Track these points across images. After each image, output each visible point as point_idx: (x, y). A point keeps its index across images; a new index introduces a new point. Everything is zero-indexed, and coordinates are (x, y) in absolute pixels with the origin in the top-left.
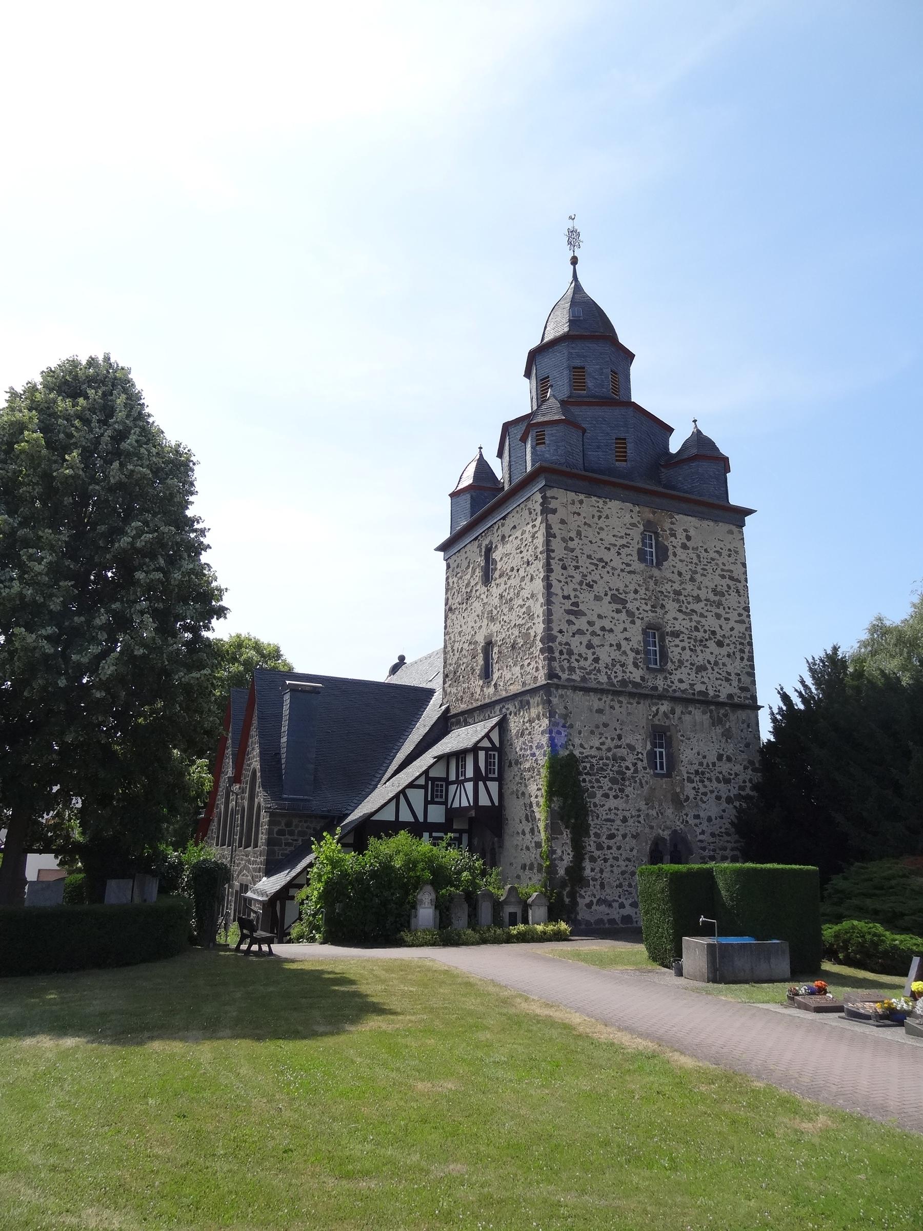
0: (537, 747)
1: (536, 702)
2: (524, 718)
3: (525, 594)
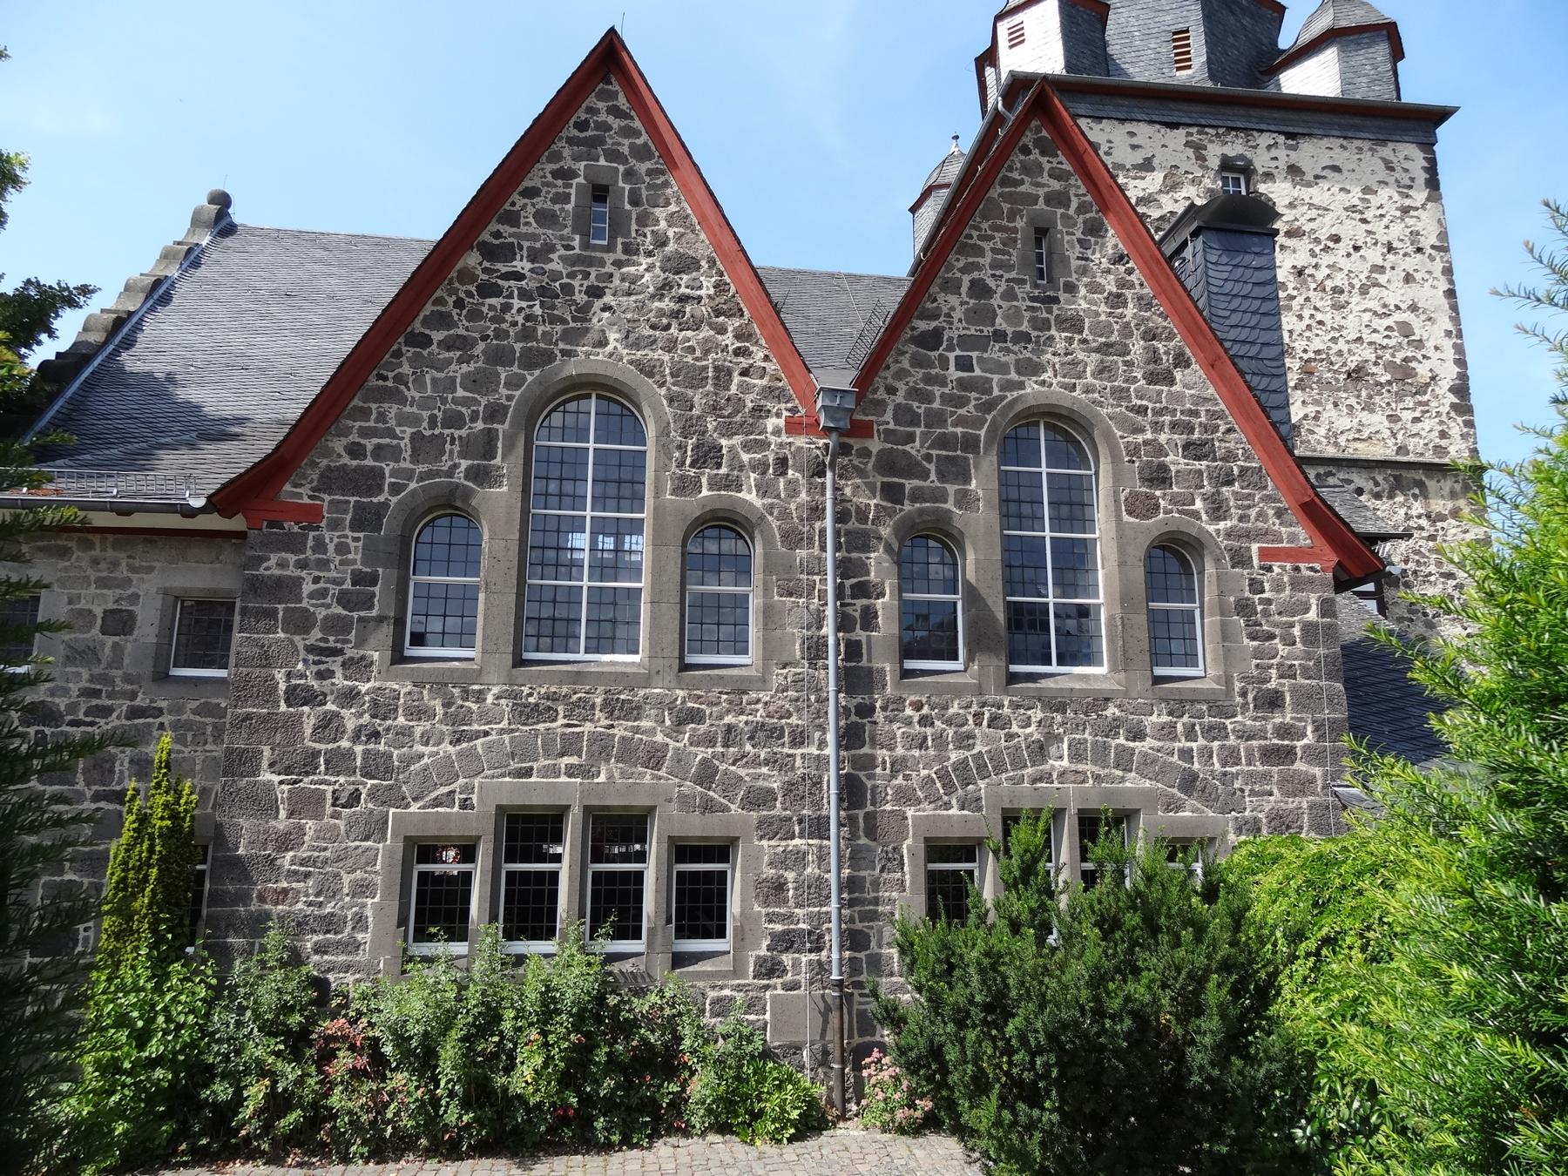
1: (1447, 489)
2: (1409, 508)
3: (1396, 293)
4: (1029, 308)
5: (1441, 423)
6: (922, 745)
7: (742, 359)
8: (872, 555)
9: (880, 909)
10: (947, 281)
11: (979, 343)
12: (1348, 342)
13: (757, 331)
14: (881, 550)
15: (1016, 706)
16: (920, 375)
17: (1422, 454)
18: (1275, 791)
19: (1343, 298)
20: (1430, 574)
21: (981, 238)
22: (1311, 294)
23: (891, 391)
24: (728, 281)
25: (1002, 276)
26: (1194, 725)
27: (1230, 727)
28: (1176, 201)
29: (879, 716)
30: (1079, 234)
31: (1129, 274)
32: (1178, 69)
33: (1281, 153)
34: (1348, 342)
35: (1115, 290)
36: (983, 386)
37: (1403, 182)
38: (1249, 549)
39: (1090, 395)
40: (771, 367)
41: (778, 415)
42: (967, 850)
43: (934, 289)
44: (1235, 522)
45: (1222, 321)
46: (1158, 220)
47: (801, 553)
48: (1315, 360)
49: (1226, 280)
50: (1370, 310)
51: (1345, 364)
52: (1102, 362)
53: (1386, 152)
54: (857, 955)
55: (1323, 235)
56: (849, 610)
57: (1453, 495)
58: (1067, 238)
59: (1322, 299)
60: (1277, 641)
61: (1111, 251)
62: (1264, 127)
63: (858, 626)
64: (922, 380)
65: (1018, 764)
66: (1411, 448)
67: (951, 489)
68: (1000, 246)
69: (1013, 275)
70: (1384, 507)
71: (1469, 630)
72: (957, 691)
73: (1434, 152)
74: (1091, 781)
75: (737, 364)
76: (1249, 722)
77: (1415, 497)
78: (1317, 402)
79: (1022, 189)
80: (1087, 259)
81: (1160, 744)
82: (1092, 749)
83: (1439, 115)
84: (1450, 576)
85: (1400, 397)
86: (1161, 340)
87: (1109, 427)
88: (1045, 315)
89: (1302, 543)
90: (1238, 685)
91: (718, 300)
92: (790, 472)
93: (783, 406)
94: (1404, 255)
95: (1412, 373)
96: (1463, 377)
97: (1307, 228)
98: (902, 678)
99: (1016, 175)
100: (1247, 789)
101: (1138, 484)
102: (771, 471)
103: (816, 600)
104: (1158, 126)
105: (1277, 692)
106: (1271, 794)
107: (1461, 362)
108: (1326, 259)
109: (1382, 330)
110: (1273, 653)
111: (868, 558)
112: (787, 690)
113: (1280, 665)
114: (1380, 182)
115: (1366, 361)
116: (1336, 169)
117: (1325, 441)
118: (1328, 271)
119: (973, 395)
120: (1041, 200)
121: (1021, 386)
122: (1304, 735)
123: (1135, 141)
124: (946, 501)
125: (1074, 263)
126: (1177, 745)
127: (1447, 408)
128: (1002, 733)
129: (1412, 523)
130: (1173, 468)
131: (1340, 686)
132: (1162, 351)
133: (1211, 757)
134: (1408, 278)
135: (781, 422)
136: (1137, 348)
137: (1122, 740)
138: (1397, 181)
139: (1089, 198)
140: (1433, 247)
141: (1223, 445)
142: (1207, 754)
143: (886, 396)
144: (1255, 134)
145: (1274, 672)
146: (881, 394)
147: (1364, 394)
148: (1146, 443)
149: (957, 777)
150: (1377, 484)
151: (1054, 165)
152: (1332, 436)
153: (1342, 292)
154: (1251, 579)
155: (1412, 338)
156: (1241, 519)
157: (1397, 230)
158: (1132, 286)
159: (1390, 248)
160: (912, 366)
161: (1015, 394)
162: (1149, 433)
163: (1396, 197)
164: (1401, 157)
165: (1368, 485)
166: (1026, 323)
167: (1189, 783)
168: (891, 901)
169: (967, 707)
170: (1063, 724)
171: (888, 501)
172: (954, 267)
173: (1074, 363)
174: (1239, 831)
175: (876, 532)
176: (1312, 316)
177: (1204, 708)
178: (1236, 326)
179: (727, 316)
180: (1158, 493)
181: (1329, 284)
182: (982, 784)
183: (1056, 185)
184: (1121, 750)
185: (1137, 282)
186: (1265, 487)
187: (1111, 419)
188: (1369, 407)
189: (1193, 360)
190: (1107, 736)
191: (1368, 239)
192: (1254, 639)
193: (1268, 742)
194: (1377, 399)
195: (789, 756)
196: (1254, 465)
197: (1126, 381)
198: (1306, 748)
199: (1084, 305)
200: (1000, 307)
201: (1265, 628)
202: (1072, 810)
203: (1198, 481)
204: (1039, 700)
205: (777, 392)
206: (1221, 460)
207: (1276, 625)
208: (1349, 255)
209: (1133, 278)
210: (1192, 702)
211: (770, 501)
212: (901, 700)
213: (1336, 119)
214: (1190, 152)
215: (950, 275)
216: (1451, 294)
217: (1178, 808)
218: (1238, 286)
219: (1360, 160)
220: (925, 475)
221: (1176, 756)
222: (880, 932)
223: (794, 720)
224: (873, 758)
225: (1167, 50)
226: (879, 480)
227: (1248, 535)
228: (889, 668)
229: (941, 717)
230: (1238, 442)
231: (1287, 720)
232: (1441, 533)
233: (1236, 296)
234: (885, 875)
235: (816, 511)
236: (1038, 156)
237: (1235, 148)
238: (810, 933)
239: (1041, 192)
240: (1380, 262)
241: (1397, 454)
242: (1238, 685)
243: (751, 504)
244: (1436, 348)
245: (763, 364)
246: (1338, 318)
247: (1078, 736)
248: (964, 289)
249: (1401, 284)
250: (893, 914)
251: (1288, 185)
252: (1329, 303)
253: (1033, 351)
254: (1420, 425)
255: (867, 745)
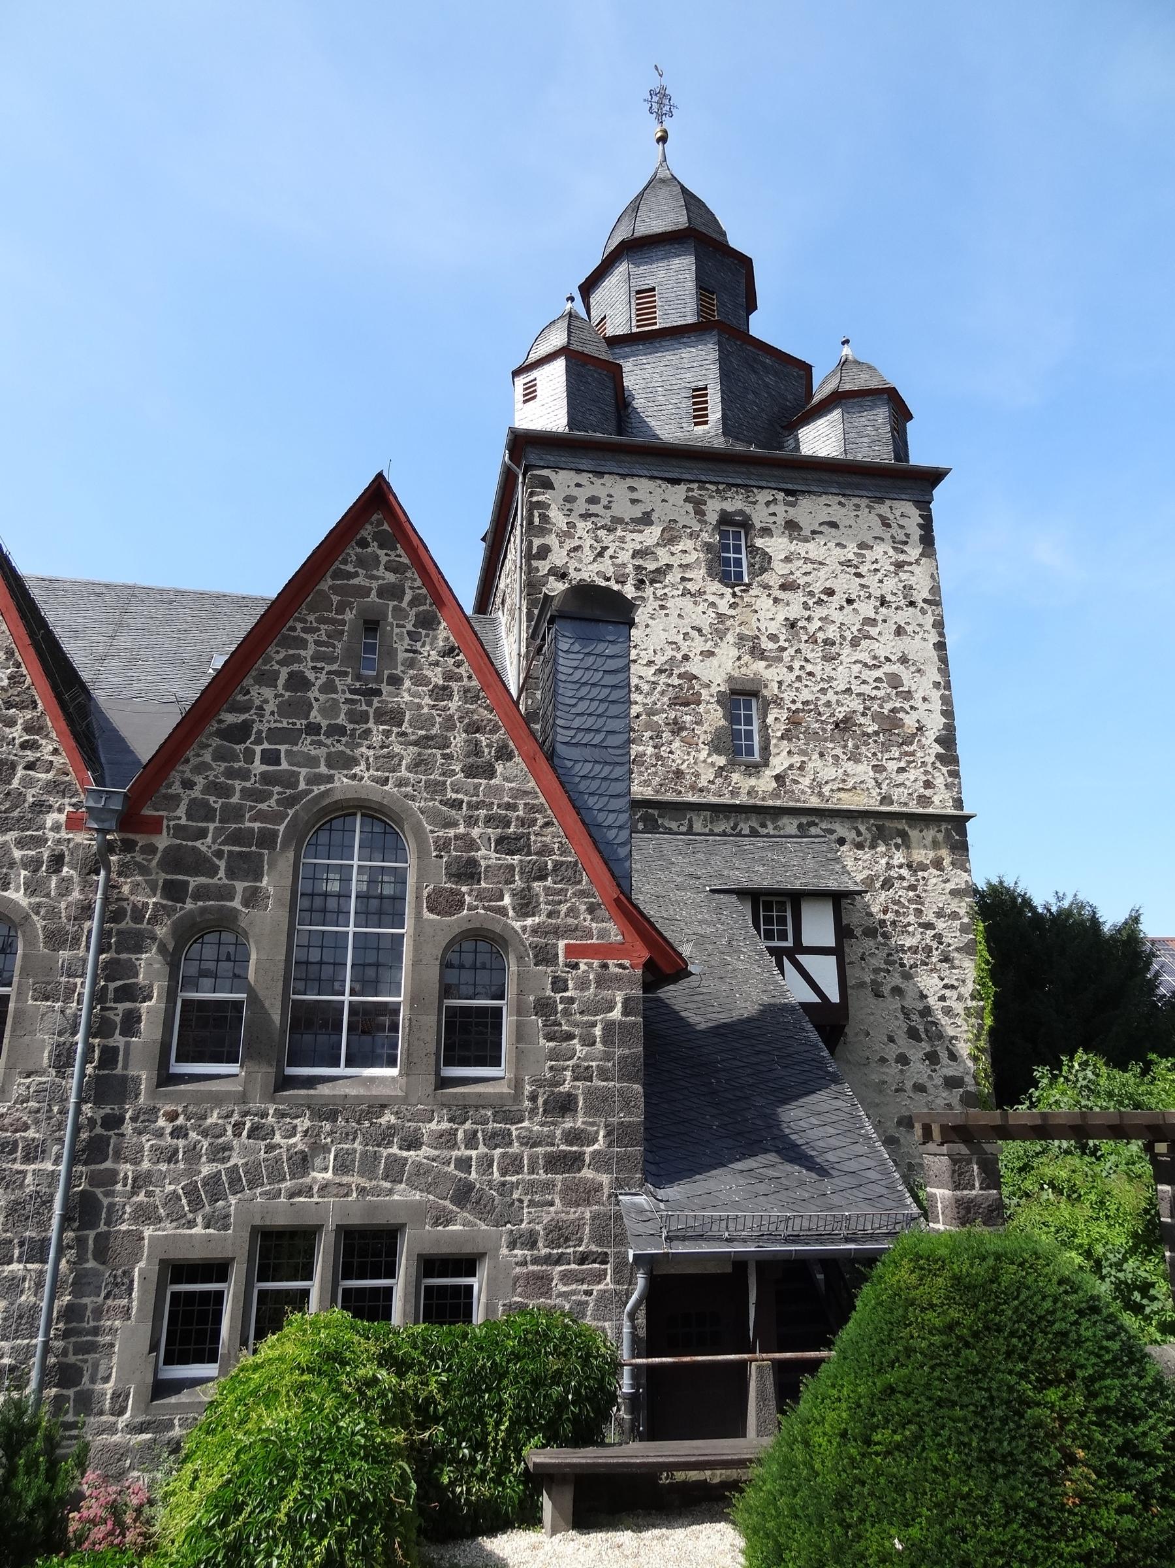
0: (940, 914)
1: (930, 839)
2: (891, 857)
3: (886, 645)
4: (347, 701)
5: (926, 772)
6: (172, 1158)
7: (29, 753)
8: (144, 956)
9: (99, 1339)
10: (263, 674)
11: (289, 736)
12: (836, 693)
13: (49, 724)
14: (154, 950)
15: (280, 1115)
16: (222, 769)
17: (906, 804)
18: (557, 1201)
19: (834, 650)
20: (909, 924)
21: (304, 630)
22: (803, 646)
23: (188, 785)
24: (25, 672)
25: (323, 669)
26: (475, 1132)
27: (515, 1133)
28: (673, 554)
29: (128, 1128)
30: (410, 627)
31: (458, 667)
32: (696, 424)
33: (780, 509)
34: (836, 693)
35: (441, 682)
36: (289, 781)
37: (898, 538)
38: (555, 946)
39: (403, 789)
40: (58, 761)
41: (60, 810)
42: (218, 1270)
43: (248, 681)
44: (543, 918)
45: (567, 709)
46: (653, 572)
47: (64, 954)
48: (803, 710)
49: (576, 668)
50: (860, 662)
51: (832, 715)
52: (419, 754)
53: (883, 509)
54: (65, 1392)
55: (817, 588)
56: (110, 1014)
57: (935, 845)
58: (396, 630)
59: (813, 650)
60: (576, 1041)
61: (441, 644)
62: (763, 484)
63: (118, 1031)
64: (223, 774)
65: (276, 1176)
66: (895, 798)
67: (240, 886)
68: (325, 638)
69: (335, 667)
70: (865, 857)
71: (946, 981)
72: (218, 1099)
73: (930, 510)
74: (354, 1195)
75: (23, 757)
76: (536, 1128)
77: (897, 847)
78: (803, 753)
79: (355, 581)
80: (415, 652)
81: (437, 1153)
82: (361, 1158)
83: (935, 476)
84: (929, 926)
85: (886, 747)
86: (483, 733)
87: (419, 822)
88: (364, 708)
89: (613, 939)
90: (528, 1089)
91: (11, 692)
92: (65, 869)
93: (67, 801)
94: (896, 609)
95: (899, 724)
96: (950, 728)
97: (801, 581)
98: (159, 1085)
99: (350, 568)
100: (526, 1199)
101: (444, 879)
102: (44, 868)
103: (75, 1004)
104: (659, 482)
105: (569, 1095)
106: (552, 1204)
107: (948, 713)
108: (819, 612)
109: (871, 681)
110: (570, 1054)
111: (138, 959)
112: (27, 1101)
113: (575, 1068)
114: (875, 538)
115: (854, 712)
116: (833, 525)
117: (809, 791)
118: (820, 624)
119: (277, 789)
120: (374, 592)
121: (330, 779)
122: (595, 1141)
123: (635, 496)
124: (232, 899)
125: (402, 655)
126: (455, 1153)
127: (933, 759)
128: (263, 1144)
129: (893, 873)
130: (483, 863)
131: (638, 1088)
132: (484, 744)
133: (490, 1165)
134: (899, 631)
135: (62, 818)
136: (458, 740)
137: (395, 1150)
138: (892, 537)
139: (424, 591)
140: (925, 601)
141: (539, 839)
142: (486, 1163)
143: (181, 791)
144: (755, 490)
145: (568, 1074)
146: (176, 789)
147: (850, 744)
148: (457, 837)
149: (206, 1192)
150: (859, 834)
151: (393, 558)
152: (817, 786)
153: (834, 644)
154: (554, 977)
155: (901, 689)
156: (550, 915)
157: (891, 584)
158: (460, 678)
159: (883, 602)
160: (214, 760)
161: (322, 788)
162: (462, 827)
163: (891, 552)
164: (898, 514)
165: (850, 835)
166: (342, 716)
167: (464, 1194)
168: (112, 1331)
169: (227, 1117)
170: (332, 1133)
171: (169, 899)
172: (273, 659)
173: (390, 756)
174: (512, 1245)
175: (152, 931)
176: (802, 667)
177: (489, 1113)
178: (582, 714)
179: (20, 709)
180: (464, 889)
181: (821, 636)
182: (233, 1200)
183: (391, 578)
184: (393, 1160)
185: (465, 675)
186: (580, 882)
187: (422, 813)
188: (855, 758)
189: (516, 753)
190: (379, 1145)
191: (862, 593)
192: (550, 1040)
193: (555, 1149)
194: (863, 749)
195: (18, 1172)
196: (569, 859)
197: (443, 774)
198: (596, 1153)
199: (407, 698)
200: (317, 700)
201: (565, 1028)
202: (330, 1226)
203: (509, 876)
204: (309, 1108)
205: (62, 787)
206: (536, 854)
207: (576, 1025)
208: (842, 608)
209: (462, 670)
210: (477, 1107)
211: (38, 899)
212: (154, 1111)
213: (835, 477)
214: (690, 507)
215: (267, 667)
216: (941, 646)
217: (448, 1222)
218: (589, 674)
219: (857, 516)
220: (213, 871)
221: (452, 1166)
222: (96, 1366)
223: (31, 1133)
224: (115, 1173)
225: (687, 405)
226: (162, 877)
227: (557, 932)
228: (145, 1076)
229: (197, 1128)
230: (553, 837)
231: (579, 1124)
232: (922, 882)
233: (585, 684)
234: (109, 1302)
235: (86, 910)
236: (376, 549)
237: (734, 504)
238: (12, 1369)
239: (375, 584)
240: (873, 616)
241: (881, 803)
242: (528, 1089)
243: (16, 904)
244: (924, 699)
245: (51, 758)
246: (828, 669)
247: (346, 1146)
248: (281, 682)
249: (892, 636)
250: (112, 1345)
251: (786, 540)
252: (820, 654)
253: (347, 745)
254: (905, 775)
255: (110, 1160)
